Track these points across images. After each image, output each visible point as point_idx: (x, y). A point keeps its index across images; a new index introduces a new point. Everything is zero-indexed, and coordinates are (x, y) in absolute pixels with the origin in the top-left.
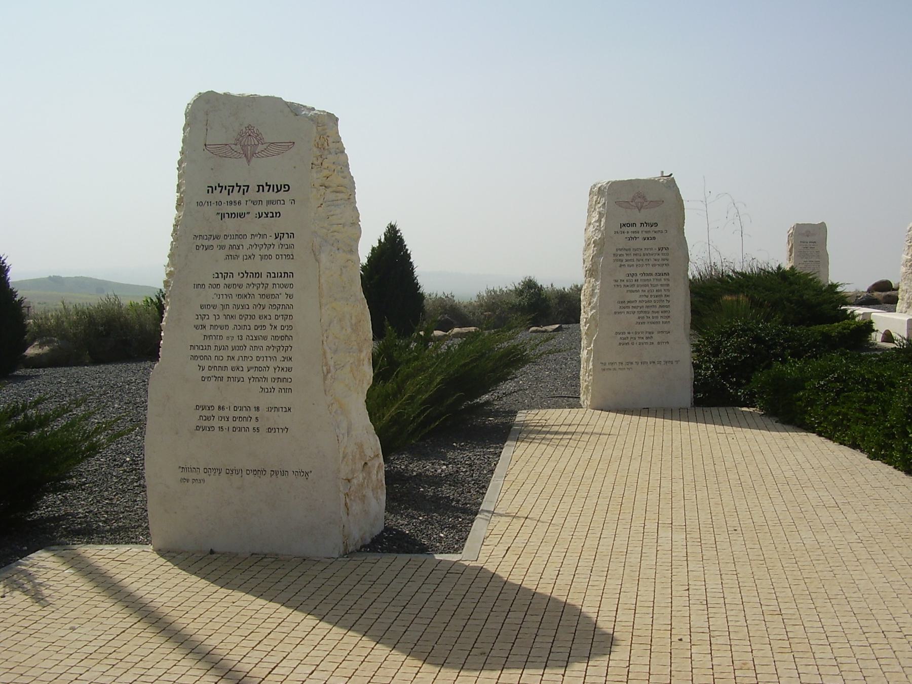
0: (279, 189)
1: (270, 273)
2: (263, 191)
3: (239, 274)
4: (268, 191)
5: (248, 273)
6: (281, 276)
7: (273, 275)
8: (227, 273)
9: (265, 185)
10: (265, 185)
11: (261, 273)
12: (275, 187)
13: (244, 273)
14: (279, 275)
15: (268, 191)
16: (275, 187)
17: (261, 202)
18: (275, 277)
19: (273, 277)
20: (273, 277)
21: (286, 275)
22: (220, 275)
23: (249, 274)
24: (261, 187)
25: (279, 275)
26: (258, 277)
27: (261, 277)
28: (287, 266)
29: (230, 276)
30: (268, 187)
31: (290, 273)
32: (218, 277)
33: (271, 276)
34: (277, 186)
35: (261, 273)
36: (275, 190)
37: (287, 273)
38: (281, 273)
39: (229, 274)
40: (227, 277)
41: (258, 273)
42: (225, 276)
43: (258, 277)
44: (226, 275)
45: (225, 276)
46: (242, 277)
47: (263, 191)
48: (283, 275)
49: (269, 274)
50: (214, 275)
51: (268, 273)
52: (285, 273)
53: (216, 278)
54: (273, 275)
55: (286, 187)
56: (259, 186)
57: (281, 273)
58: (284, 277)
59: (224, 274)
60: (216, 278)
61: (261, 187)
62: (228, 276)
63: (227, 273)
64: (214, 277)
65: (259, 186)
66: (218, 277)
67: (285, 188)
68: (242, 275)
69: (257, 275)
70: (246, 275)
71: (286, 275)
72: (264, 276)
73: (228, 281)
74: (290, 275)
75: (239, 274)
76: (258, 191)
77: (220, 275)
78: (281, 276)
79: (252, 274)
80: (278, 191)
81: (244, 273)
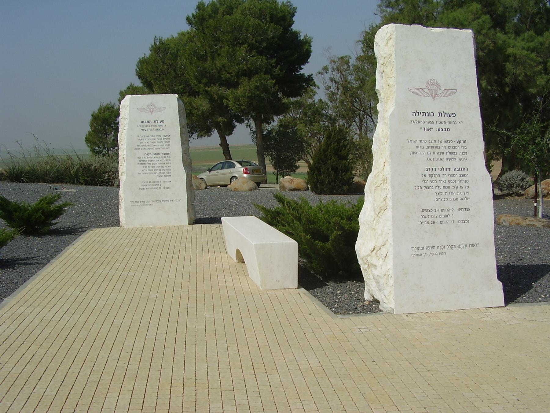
0: (450, 115)
2: (442, 116)
4: (445, 116)
6: (461, 170)
7: (457, 169)
9: (442, 113)
10: (442, 113)
12: (448, 114)
14: (461, 169)
15: (445, 116)
16: (448, 114)
23: (445, 169)
24: (440, 114)
25: (461, 169)
28: (465, 164)
30: (444, 114)
34: (449, 113)
36: (448, 116)
38: (461, 168)
47: (442, 116)
48: (462, 170)
54: (457, 169)
55: (454, 114)
56: (439, 113)
61: (440, 114)
65: (439, 113)
67: (453, 115)
68: (441, 169)
69: (449, 169)
72: (453, 169)
76: (439, 116)
78: (461, 170)
80: (450, 116)
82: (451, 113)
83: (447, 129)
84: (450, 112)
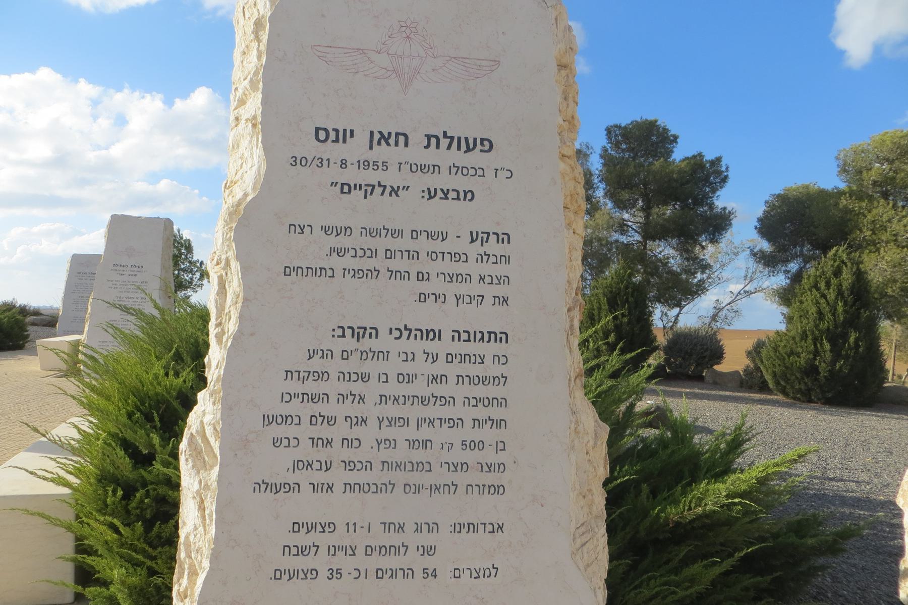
1: (458, 332)
3: (391, 329)
5: (410, 330)
6: (482, 339)
7: (464, 336)
8: (365, 329)
11: (440, 331)
13: (403, 329)
14: (479, 336)
17: (436, 168)
18: (469, 340)
19: (464, 341)
20: (464, 341)
21: (493, 336)
22: (348, 332)
25: (479, 336)
26: (432, 340)
27: (439, 339)
29: (371, 334)
31: (501, 333)
32: (344, 336)
33: (462, 339)
35: (440, 331)
37: (495, 333)
39: (368, 331)
40: (363, 337)
41: (433, 330)
42: (358, 333)
43: (432, 340)
44: (362, 331)
45: (358, 333)
46: (396, 338)
49: (456, 335)
50: (334, 330)
51: (453, 331)
52: (490, 333)
53: (339, 336)
54: (464, 336)
57: (482, 333)
58: (489, 341)
59: (356, 331)
60: (339, 336)
62: (367, 335)
63: (365, 329)
64: (333, 336)
66: (344, 336)
68: (396, 334)
69: (431, 334)
70: (406, 334)
71: (493, 336)
73: (367, 343)
74: (501, 338)
75: (391, 329)
77: (348, 332)
78: (482, 339)
79: (419, 333)
81: (403, 329)
82: (475, 140)
83: (465, 193)
84: (472, 134)
